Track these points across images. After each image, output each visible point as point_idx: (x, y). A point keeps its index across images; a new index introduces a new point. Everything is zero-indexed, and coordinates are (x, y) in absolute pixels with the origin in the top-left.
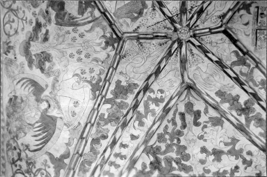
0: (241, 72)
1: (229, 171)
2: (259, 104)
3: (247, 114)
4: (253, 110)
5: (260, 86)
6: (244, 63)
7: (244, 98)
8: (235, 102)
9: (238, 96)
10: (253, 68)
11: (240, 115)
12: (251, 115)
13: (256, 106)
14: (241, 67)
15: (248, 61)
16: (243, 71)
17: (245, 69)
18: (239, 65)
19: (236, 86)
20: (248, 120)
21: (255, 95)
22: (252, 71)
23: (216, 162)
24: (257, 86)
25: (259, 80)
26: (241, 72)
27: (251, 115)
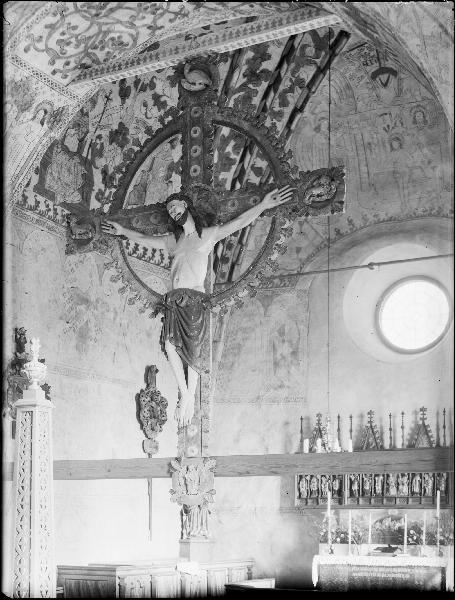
0: (304, 47)
1: (168, 108)
2: (269, 88)
3: (249, 81)
4: (258, 85)
5: (294, 79)
6: (318, 48)
7: (270, 65)
8: (259, 60)
9: (270, 56)
10: (315, 63)
11: (244, 76)
12: (251, 86)
13: (265, 85)
14: (312, 44)
15: (323, 53)
16: (308, 50)
17: (310, 51)
18: (314, 41)
19: (283, 48)
20: (243, 87)
21: (277, 81)
22: (310, 62)
23: (168, 83)
24: (293, 75)
25: (302, 77)
26: (304, 47)
27: (251, 86)
